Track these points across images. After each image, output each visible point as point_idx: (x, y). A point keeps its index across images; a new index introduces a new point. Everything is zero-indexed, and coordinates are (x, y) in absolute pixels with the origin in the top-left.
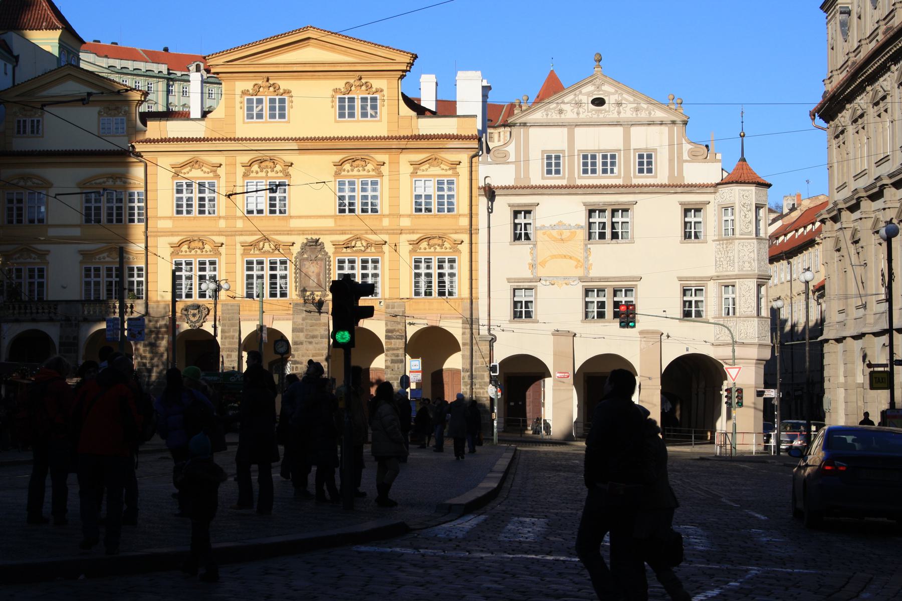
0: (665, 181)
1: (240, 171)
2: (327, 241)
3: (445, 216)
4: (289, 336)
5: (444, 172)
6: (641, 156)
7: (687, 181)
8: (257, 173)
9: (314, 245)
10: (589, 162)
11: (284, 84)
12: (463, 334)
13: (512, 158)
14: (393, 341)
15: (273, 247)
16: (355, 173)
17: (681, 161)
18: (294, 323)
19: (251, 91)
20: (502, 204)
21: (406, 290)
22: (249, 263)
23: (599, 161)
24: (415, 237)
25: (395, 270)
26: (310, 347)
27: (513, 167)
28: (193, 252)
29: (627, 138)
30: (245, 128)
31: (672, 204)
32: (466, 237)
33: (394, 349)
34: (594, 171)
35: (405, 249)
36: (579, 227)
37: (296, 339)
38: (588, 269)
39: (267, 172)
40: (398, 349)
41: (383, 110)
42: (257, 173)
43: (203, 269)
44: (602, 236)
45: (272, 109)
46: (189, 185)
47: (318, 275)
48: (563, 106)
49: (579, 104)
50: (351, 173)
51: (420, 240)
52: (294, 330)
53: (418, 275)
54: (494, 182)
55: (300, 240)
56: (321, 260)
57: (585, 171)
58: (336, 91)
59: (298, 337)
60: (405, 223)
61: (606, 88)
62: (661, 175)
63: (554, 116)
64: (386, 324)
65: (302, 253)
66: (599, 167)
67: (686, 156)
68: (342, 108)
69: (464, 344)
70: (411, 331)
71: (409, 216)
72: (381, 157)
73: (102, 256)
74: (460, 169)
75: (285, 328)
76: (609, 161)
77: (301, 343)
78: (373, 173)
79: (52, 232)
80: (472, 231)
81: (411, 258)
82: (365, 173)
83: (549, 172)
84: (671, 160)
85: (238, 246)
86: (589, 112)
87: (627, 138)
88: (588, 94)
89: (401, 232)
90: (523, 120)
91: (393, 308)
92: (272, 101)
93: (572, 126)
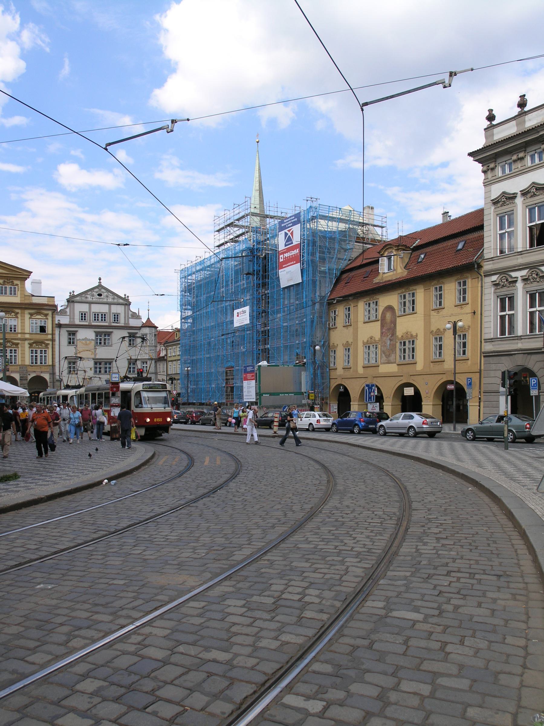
0: (123, 325)
6: (115, 315)
7: (131, 325)
10: (96, 316)
13: (68, 314)
16: (7, 316)
17: (129, 318)
20: (64, 331)
21: (28, 362)
23: (100, 316)
27: (68, 317)
29: (110, 309)
31: (125, 333)
32: (50, 343)
34: (98, 320)
35: (27, 346)
36: (92, 340)
38: (95, 355)
41: (19, 293)
44: (100, 343)
48: (88, 296)
49: (93, 295)
51: (34, 343)
53: (32, 356)
54: (61, 323)
57: (95, 320)
60: (27, 336)
61: (103, 290)
62: (122, 322)
63: (84, 299)
66: (100, 318)
67: (130, 317)
69: (50, 382)
70: (29, 377)
72: (17, 311)
76: (104, 316)
80: (53, 340)
83: (82, 319)
84: (125, 317)
86: (96, 298)
87: (110, 309)
88: (96, 292)
89: (26, 339)
90: (73, 300)
93: (90, 303)
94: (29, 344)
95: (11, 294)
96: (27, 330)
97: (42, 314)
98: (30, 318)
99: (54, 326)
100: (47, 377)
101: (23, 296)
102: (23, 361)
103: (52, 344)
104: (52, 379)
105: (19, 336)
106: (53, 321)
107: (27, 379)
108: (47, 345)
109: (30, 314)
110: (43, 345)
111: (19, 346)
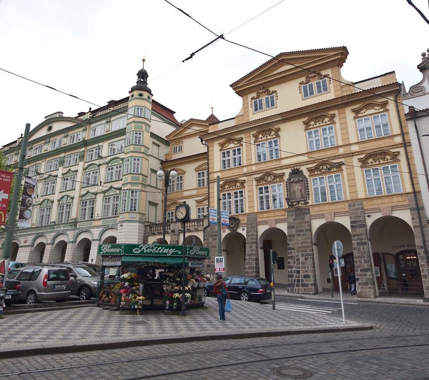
1: (253, 139)
2: (304, 169)
3: (383, 138)
4: (286, 231)
5: (377, 111)
8: (261, 138)
9: (296, 172)
11: (272, 89)
12: (413, 219)
14: (357, 230)
15: (273, 178)
16: (318, 125)
18: (288, 223)
19: (256, 97)
22: (261, 189)
24: (363, 156)
25: (352, 180)
26: (299, 238)
28: (231, 188)
30: (253, 116)
32: (402, 150)
33: (358, 235)
37: (290, 234)
39: (267, 137)
40: (361, 235)
41: (331, 86)
42: (261, 138)
43: (237, 197)
45: (267, 102)
46: (228, 152)
47: (301, 190)
50: (315, 126)
52: (288, 228)
55: (287, 172)
56: (302, 181)
58: (301, 83)
59: (291, 232)
60: (355, 148)
64: (351, 218)
65: (289, 179)
68: (305, 91)
69: (415, 227)
70: (369, 222)
71: (357, 143)
72: (331, 112)
73: (205, 202)
74: (388, 107)
75: (283, 227)
77: (294, 236)
78: (329, 123)
79: (186, 194)
80: (406, 144)
81: (362, 170)
82: (324, 124)
85: (254, 180)
89: (353, 154)
91: (354, 205)
92: (267, 99)
94: (360, 160)
95: (319, 91)
96: (353, 139)
97: (376, 105)
98: (355, 118)
99: (403, 118)
100: (406, 216)
101: (340, 88)
102: (354, 191)
103: (406, 153)
104: (417, 220)
105: (341, 151)
106: (398, 111)
107: (364, 226)
108: (395, 156)
109: (353, 111)
110: (388, 157)
111: (344, 167)
